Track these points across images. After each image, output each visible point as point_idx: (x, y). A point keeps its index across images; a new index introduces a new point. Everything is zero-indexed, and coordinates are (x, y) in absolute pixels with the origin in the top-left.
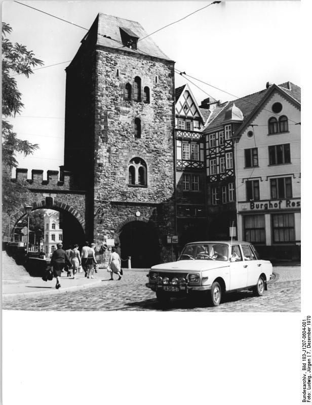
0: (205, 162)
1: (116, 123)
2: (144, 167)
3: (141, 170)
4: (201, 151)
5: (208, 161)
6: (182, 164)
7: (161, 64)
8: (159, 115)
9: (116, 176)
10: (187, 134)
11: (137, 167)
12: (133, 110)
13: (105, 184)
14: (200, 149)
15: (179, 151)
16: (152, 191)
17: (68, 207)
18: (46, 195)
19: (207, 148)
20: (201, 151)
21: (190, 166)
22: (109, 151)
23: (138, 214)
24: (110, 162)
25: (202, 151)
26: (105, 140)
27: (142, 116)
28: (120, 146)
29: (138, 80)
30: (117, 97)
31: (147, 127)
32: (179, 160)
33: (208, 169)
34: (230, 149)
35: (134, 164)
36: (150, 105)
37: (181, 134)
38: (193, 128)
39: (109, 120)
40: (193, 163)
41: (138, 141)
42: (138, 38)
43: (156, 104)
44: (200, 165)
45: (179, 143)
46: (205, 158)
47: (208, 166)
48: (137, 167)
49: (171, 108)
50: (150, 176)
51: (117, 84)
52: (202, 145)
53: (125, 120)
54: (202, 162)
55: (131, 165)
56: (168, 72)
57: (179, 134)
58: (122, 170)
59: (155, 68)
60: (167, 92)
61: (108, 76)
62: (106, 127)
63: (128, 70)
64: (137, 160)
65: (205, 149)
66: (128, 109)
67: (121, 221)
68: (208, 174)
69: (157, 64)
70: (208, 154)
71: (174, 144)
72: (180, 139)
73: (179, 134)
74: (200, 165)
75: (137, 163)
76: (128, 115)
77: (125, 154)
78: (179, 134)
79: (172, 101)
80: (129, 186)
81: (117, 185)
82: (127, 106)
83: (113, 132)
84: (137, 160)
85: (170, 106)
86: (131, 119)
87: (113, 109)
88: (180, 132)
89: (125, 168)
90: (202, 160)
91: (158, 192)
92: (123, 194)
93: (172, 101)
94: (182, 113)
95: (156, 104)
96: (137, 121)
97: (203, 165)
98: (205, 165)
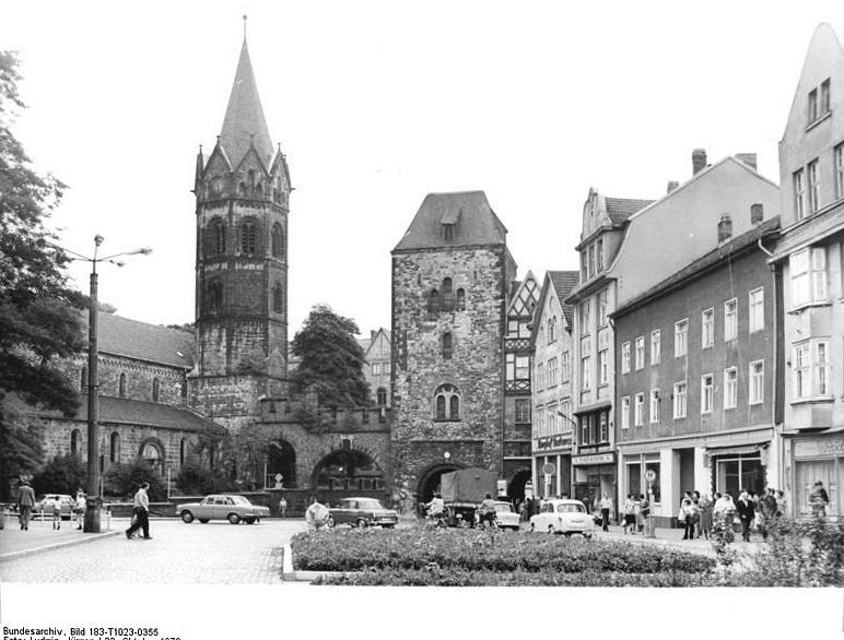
1: (417, 345)
3: (454, 398)
6: (515, 385)
7: (484, 252)
8: (479, 324)
11: (447, 395)
13: (404, 421)
15: (510, 368)
16: (466, 425)
17: (366, 450)
18: (343, 437)
22: (408, 380)
23: (447, 455)
24: (409, 393)
28: (422, 372)
29: (448, 280)
30: (419, 311)
31: (461, 343)
39: (409, 342)
41: (448, 362)
43: (474, 309)
49: (499, 310)
50: (462, 406)
51: (420, 294)
53: (431, 338)
58: (425, 401)
59: (474, 259)
60: (493, 288)
61: (407, 285)
62: (405, 351)
63: (435, 271)
66: (433, 323)
67: (424, 464)
69: (478, 252)
76: (433, 332)
77: (429, 382)
79: (500, 301)
80: (435, 421)
81: (418, 421)
82: (431, 320)
83: (414, 356)
84: (447, 387)
85: (496, 307)
86: (438, 336)
87: (414, 326)
89: (429, 399)
91: (477, 426)
92: (427, 432)
93: (500, 301)
95: (474, 309)
96: (447, 337)
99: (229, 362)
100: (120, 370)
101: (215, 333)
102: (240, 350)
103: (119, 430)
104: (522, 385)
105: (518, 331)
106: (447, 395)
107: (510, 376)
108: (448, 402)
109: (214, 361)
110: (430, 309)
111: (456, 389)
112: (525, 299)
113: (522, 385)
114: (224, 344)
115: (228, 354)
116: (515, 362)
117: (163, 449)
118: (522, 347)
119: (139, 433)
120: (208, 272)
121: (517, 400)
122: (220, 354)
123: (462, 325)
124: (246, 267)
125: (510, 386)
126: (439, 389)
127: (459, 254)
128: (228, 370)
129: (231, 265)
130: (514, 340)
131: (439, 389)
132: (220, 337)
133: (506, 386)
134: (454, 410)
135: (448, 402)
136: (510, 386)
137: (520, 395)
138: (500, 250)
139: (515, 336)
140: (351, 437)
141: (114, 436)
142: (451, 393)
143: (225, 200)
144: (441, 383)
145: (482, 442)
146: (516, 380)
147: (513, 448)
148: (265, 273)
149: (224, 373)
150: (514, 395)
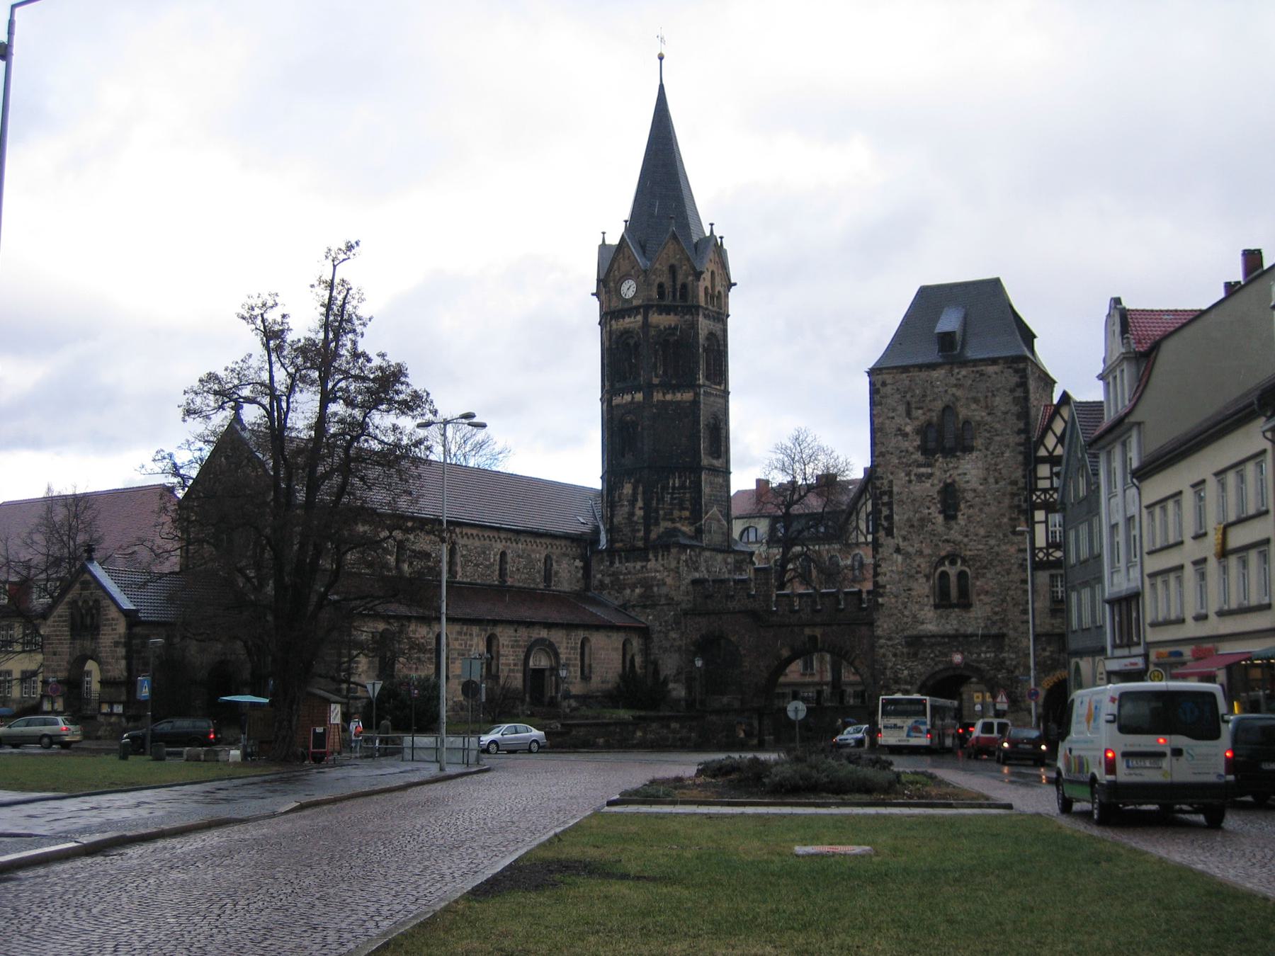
2: (967, 570)
3: (962, 575)
6: (1048, 555)
9: (913, 593)
10: (1055, 496)
12: (941, 470)
15: (1040, 530)
18: (807, 631)
26: (889, 532)
27: (957, 478)
32: (1041, 549)
35: (946, 567)
36: (975, 454)
45: (1039, 515)
51: (908, 429)
55: (943, 568)
56: (1015, 379)
66: (929, 470)
71: (1032, 523)
73: (1038, 497)
75: (953, 563)
78: (1038, 497)
89: (927, 577)
93: (1023, 436)
99: (647, 531)
100: (499, 546)
101: (627, 489)
102: (661, 512)
103: (498, 630)
106: (952, 571)
107: (1041, 541)
109: (626, 530)
110: (924, 449)
111: (964, 561)
112: (1059, 433)
113: (1058, 554)
114: (640, 504)
115: (646, 518)
116: (1046, 522)
117: (557, 655)
119: (523, 633)
120: (618, 406)
121: (1052, 576)
122: (635, 518)
123: (969, 471)
124: (669, 397)
125: (1041, 555)
126: (941, 562)
127: (964, 372)
128: (646, 538)
129: (649, 396)
130: (1045, 491)
131: (941, 562)
132: (635, 494)
134: (964, 592)
136: (1041, 555)
138: (1022, 366)
140: (818, 632)
141: (490, 641)
142: (959, 566)
143: (637, 308)
144: (943, 553)
145: (1003, 636)
146: (1049, 546)
148: (695, 403)
149: (640, 544)
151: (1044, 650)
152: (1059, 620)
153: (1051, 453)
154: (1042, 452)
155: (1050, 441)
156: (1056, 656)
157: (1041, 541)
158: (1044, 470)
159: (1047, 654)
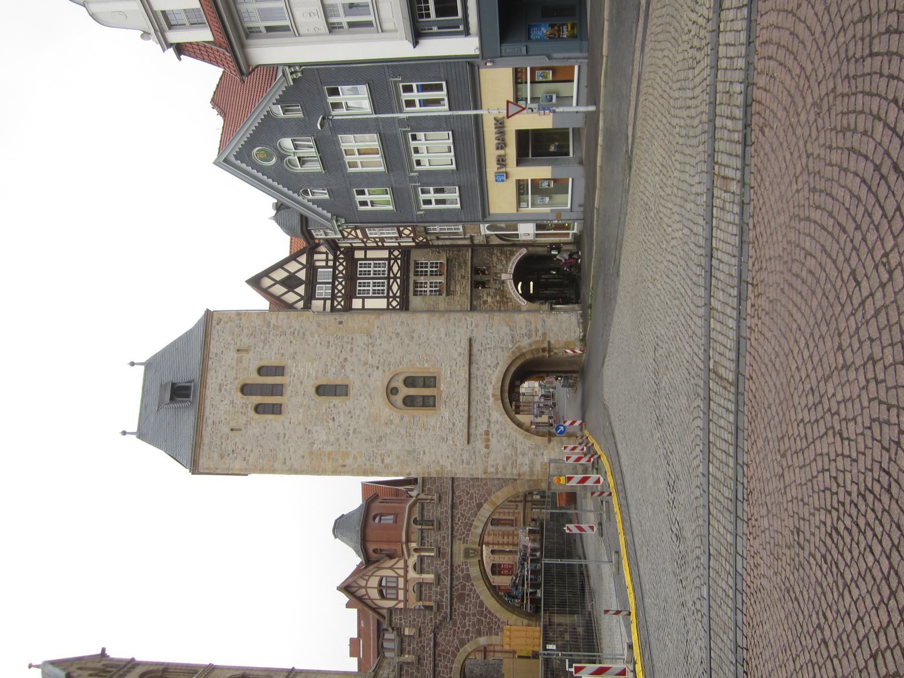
0: (391, 249)
4: (368, 256)
5: (386, 244)
6: (394, 297)
10: (340, 287)
14: (365, 259)
15: (370, 304)
19: (363, 245)
20: (368, 256)
21: (398, 281)
25: (371, 254)
32: (389, 304)
33: (402, 244)
34: (359, 231)
37: (339, 300)
38: (327, 267)
40: (392, 275)
42: (173, 384)
44: (396, 259)
45: (357, 303)
46: (383, 248)
47: (397, 244)
48: (405, 391)
52: (359, 254)
54: (390, 253)
57: (340, 303)
64: (392, 391)
65: (366, 249)
68: (413, 244)
70: (375, 245)
72: (350, 295)
74: (396, 259)
78: (339, 303)
88: (336, 303)
90: (385, 254)
94: (301, 290)
97: (396, 253)
98: (395, 248)
104: (395, 288)
105: (325, 300)
107: (382, 303)
108: (412, 391)
113: (395, 288)
118: (344, 287)
125: (394, 303)
133: (394, 308)
135: (412, 391)
136: (394, 303)
137: (408, 291)
139: (329, 303)
146: (388, 297)
147: (479, 298)
150: (407, 297)
151: (485, 302)
152: (458, 287)
153: (302, 298)
154: (301, 304)
155: (291, 297)
156: (492, 291)
157: (382, 303)
158: (317, 304)
159: (489, 299)
